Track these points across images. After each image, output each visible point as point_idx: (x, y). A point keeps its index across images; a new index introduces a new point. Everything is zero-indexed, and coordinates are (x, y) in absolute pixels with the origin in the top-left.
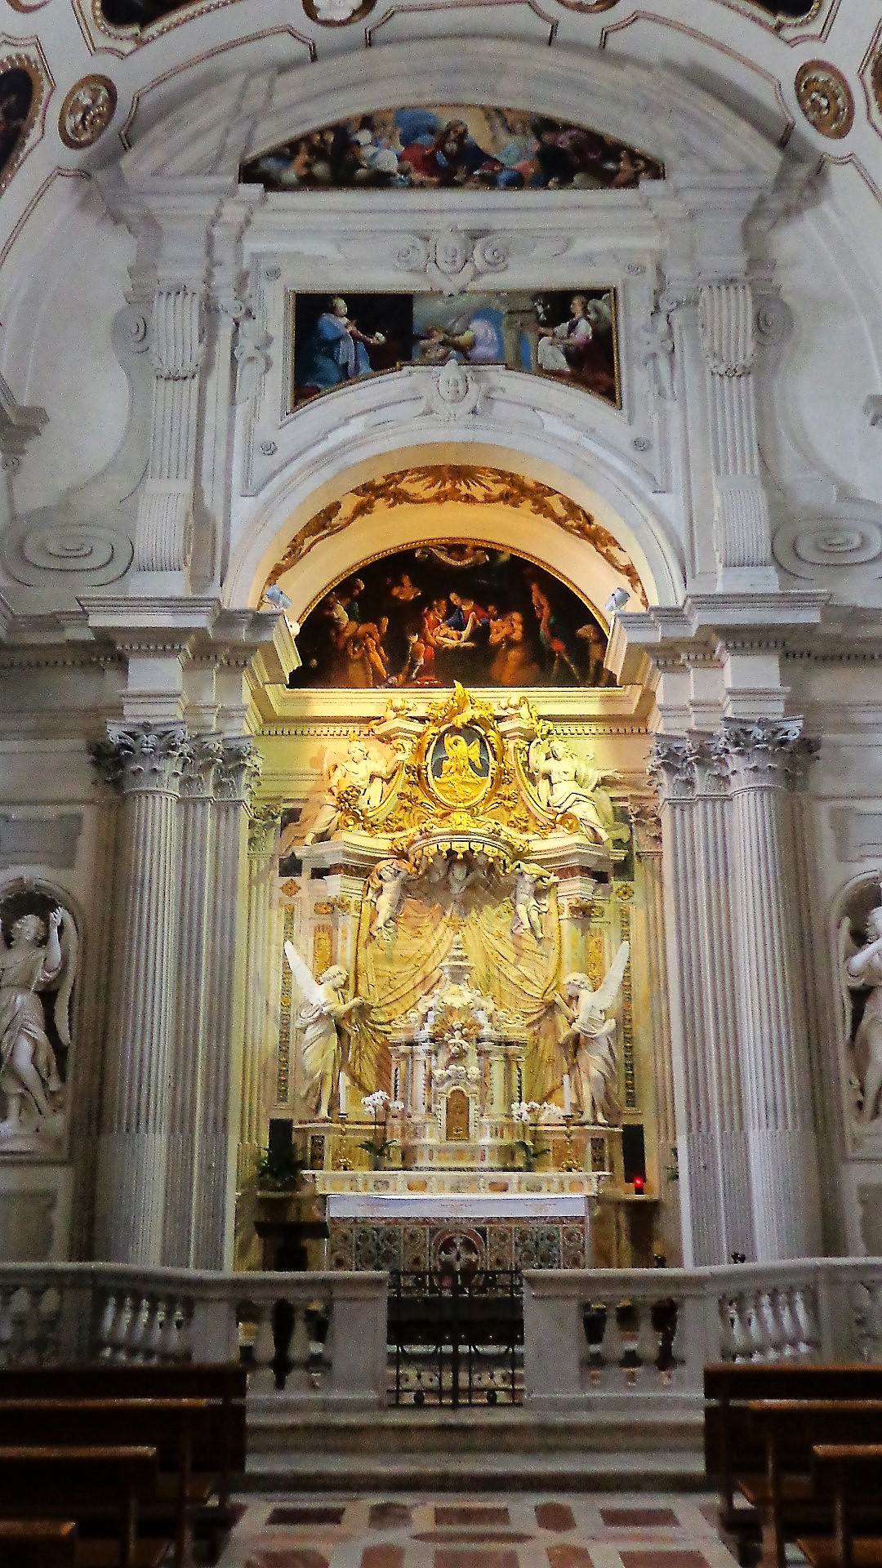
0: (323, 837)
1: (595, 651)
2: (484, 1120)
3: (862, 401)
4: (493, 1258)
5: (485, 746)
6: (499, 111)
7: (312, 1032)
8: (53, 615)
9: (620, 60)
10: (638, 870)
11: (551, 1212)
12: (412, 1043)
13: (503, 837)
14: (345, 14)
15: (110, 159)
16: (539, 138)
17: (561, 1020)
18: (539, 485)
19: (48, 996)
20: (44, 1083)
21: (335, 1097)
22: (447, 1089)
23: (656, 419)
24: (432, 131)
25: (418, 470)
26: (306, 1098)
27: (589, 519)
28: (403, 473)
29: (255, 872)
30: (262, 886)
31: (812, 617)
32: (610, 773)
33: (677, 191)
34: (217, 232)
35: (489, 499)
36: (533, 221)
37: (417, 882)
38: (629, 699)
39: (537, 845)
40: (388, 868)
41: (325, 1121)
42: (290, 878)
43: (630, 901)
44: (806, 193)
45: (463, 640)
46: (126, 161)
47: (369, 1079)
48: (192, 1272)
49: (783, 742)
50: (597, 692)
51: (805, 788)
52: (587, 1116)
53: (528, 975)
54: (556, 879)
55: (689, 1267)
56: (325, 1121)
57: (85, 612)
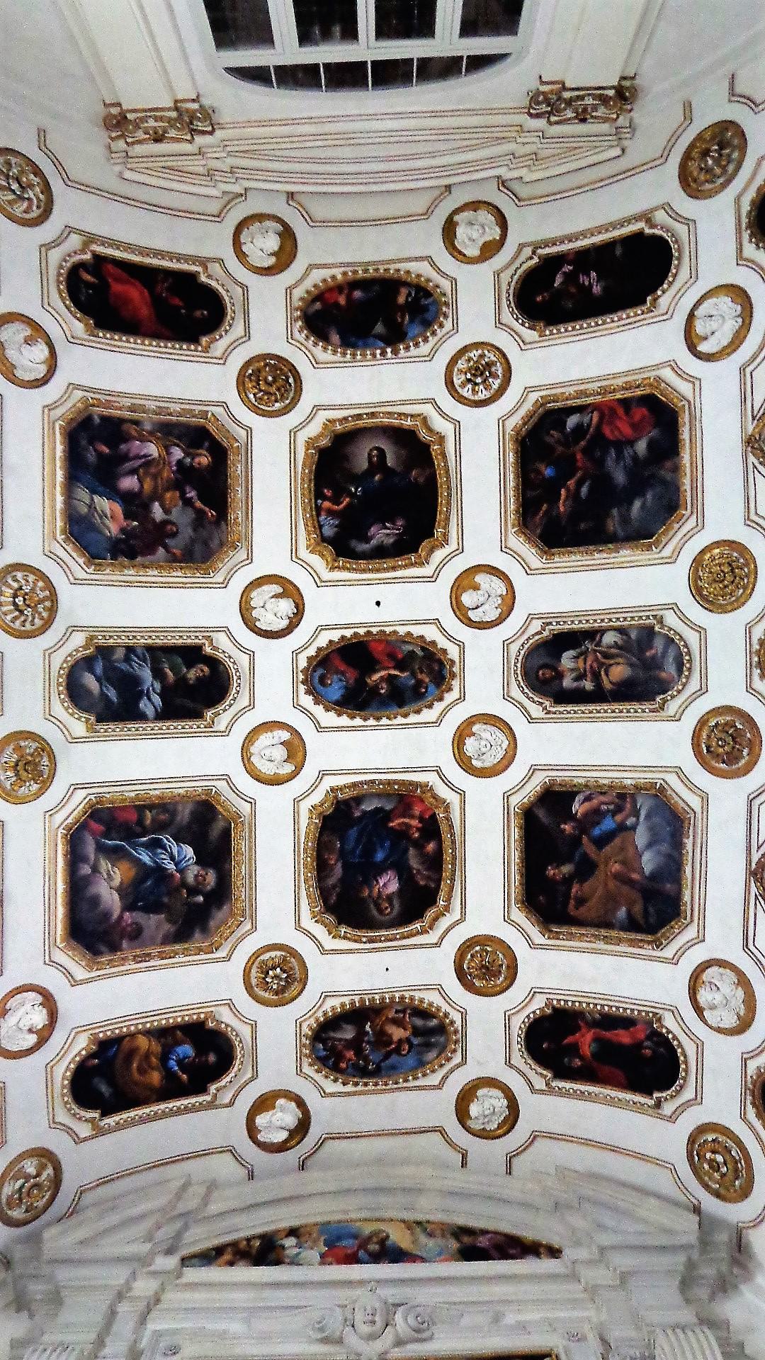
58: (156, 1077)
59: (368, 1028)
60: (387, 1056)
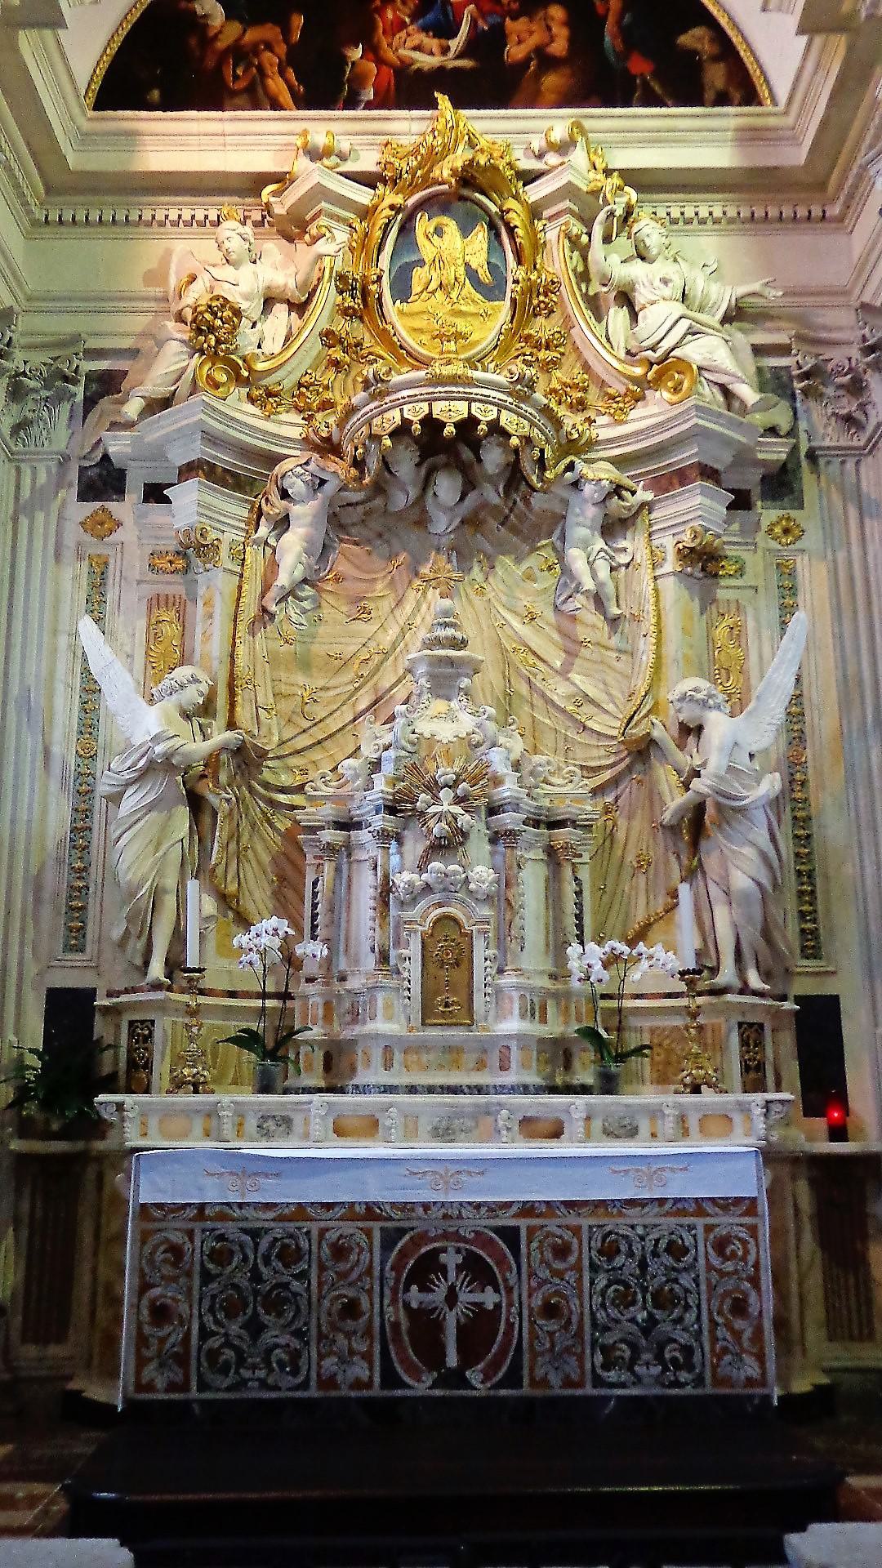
0: (159, 405)
4: (537, 1301)
5: (498, 236)
7: (132, 801)
11: (680, 1187)
12: (347, 825)
17: (666, 778)
21: (179, 937)
22: (423, 914)
29: (26, 493)
30: (40, 517)
37: (360, 509)
41: (157, 986)
42: (98, 504)
43: (799, 545)
45: (451, 54)
47: (257, 893)
52: (727, 974)
53: (592, 692)
54: (649, 496)
56: (157, 986)
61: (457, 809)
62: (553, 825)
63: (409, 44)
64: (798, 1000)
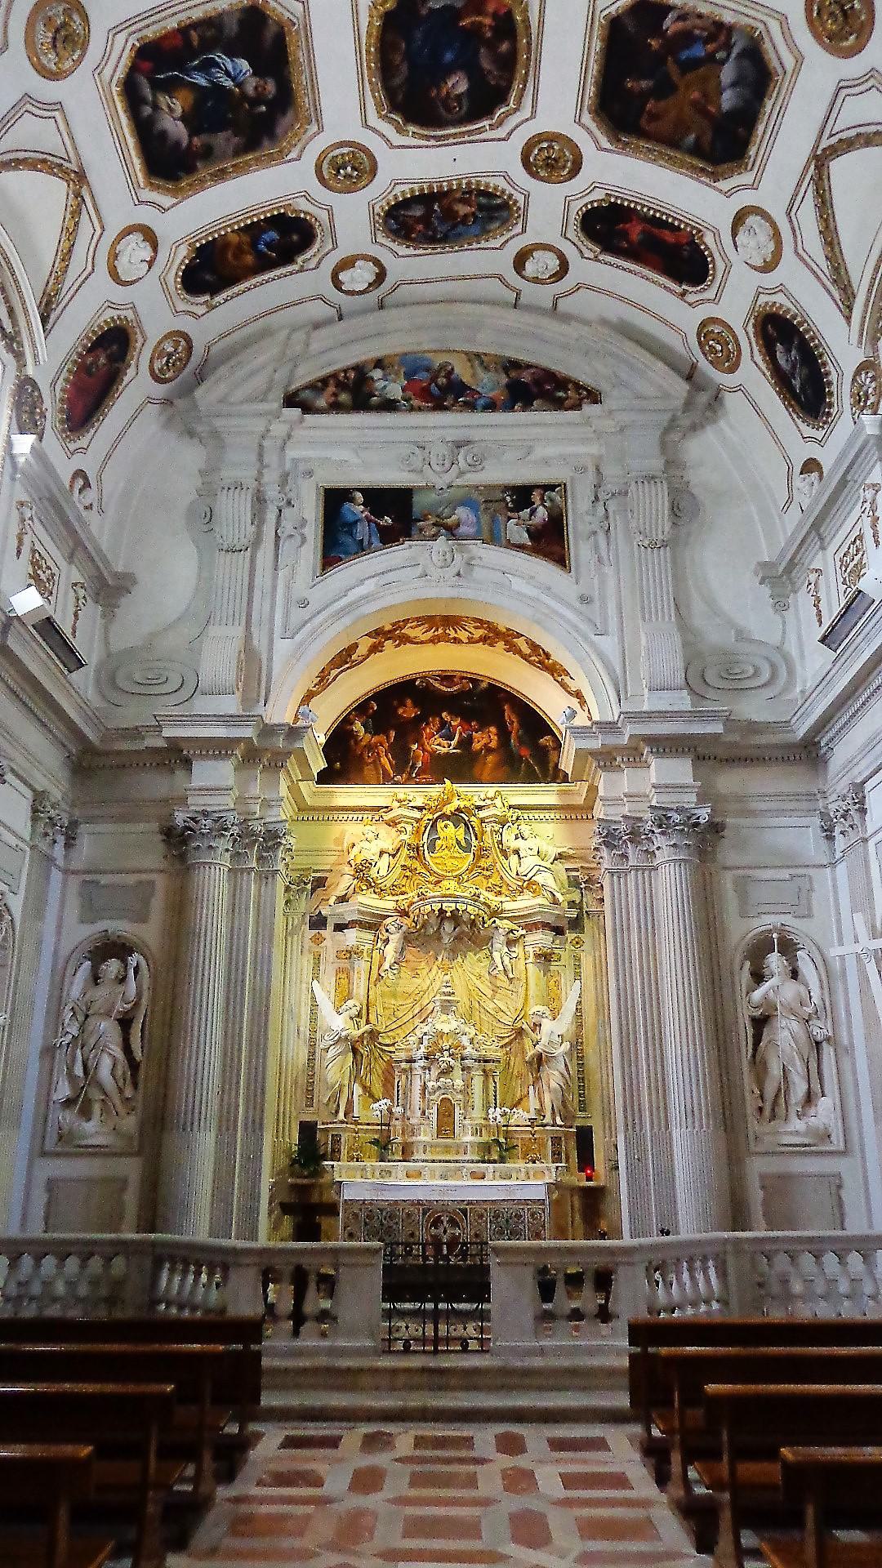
0: (343, 899)
1: (553, 755)
2: (467, 1122)
3: (753, 567)
5: (468, 828)
6: (478, 355)
7: (332, 1052)
8: (136, 728)
9: (567, 318)
10: (587, 923)
12: (411, 1061)
13: (482, 899)
14: (362, 287)
15: (188, 390)
16: (508, 375)
17: (528, 1043)
18: (508, 630)
19: (125, 1023)
20: (121, 1091)
21: (350, 1103)
22: (437, 1097)
23: (596, 581)
24: (428, 369)
25: (417, 619)
26: (327, 1105)
27: (548, 656)
28: (406, 621)
29: (290, 927)
31: (718, 728)
32: (565, 850)
33: (611, 412)
34: (266, 443)
35: (471, 641)
36: (502, 435)
38: (578, 792)
39: (507, 906)
40: (393, 923)
44: (708, 414)
46: (199, 393)
47: (377, 1089)
48: (233, 1242)
49: (697, 825)
50: (554, 786)
51: (714, 860)
54: (524, 932)
55: (627, 1241)
57: (160, 726)
58: (249, 259)
59: (436, 207)
60: (454, 227)
61: (450, 1059)
62: (486, 1061)
63: (436, 743)
64: (577, 1127)
